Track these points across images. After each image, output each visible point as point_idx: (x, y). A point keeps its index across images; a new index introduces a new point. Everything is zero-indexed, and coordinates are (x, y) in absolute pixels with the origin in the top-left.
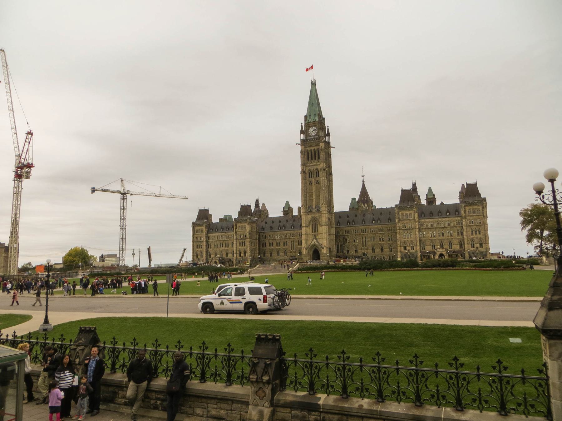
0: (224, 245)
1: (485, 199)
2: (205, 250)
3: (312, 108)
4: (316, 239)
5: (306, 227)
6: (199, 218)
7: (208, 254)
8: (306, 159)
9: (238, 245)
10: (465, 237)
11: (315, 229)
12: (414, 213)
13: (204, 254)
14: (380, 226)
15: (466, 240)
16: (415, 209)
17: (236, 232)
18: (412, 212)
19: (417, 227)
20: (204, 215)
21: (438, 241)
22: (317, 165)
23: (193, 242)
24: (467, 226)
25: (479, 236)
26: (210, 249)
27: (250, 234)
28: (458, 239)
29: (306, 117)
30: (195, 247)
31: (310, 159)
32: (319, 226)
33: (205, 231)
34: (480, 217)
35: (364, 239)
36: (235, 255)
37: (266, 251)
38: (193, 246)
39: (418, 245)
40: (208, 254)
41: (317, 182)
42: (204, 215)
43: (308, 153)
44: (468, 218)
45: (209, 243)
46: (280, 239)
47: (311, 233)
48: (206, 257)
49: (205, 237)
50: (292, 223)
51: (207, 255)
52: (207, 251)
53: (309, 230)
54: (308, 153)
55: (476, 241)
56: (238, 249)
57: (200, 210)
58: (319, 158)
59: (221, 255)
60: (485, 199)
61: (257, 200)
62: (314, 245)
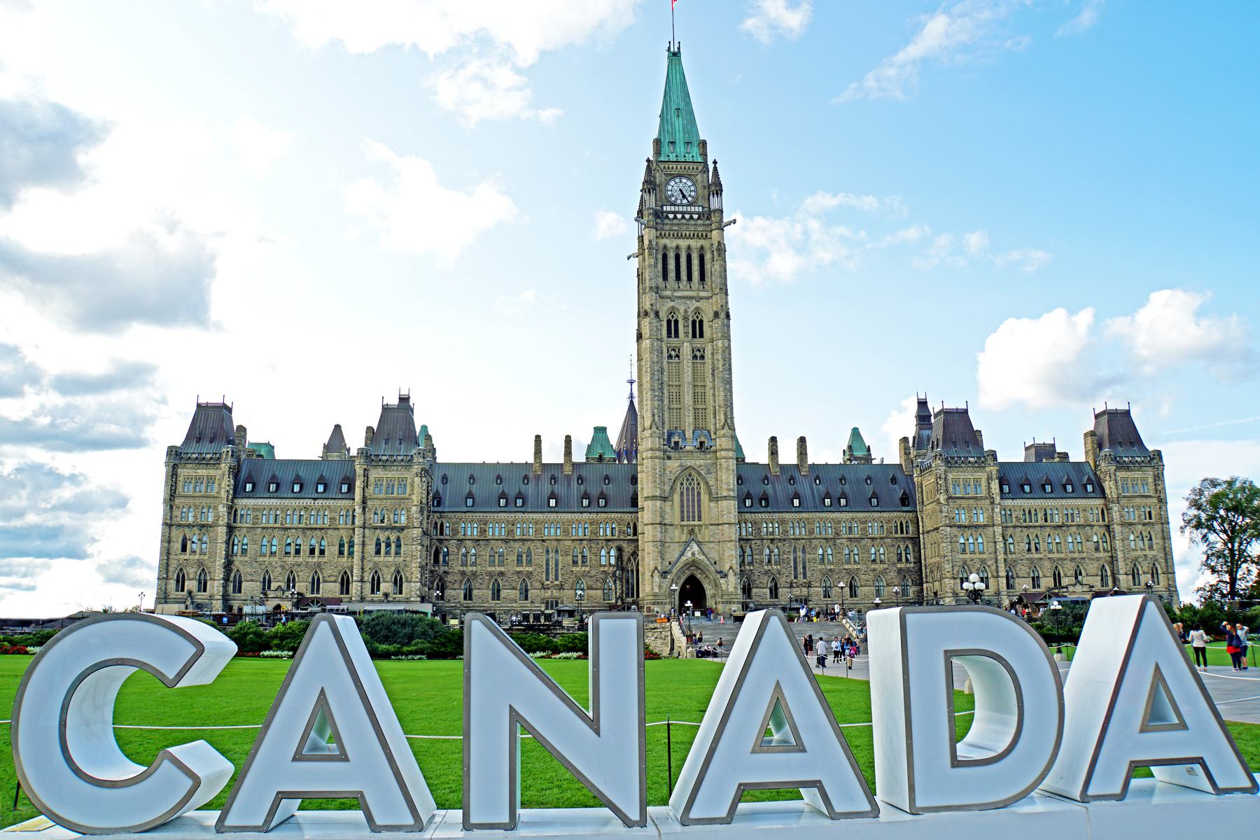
0: (305, 549)
1: (1158, 454)
2: (220, 561)
3: (679, 123)
4: (699, 544)
5: (664, 499)
6: (195, 434)
7: (232, 579)
8: (660, 274)
9: (371, 548)
10: (1120, 555)
11: (691, 510)
12: (989, 479)
13: (219, 573)
14: (851, 515)
15: (1121, 564)
16: (993, 470)
17: (364, 501)
18: (983, 476)
19: (998, 519)
20: (212, 424)
21: (1047, 564)
22: (699, 299)
23: (168, 525)
24: (1122, 524)
25: (1147, 552)
26: (238, 560)
27: (421, 511)
28: (1098, 559)
29: (657, 142)
30: (177, 546)
31: (672, 275)
32: (705, 498)
33: (227, 483)
34: (1149, 501)
35: (799, 554)
36: (355, 588)
37: (449, 578)
38: (167, 540)
39: (1003, 573)
40: (232, 579)
41: (698, 356)
42: (212, 424)
43: (665, 257)
44: (1123, 501)
45: (240, 538)
46: (506, 541)
47: (677, 521)
48: (225, 587)
49: (222, 510)
50: (546, 488)
51: (226, 579)
52: (228, 566)
53: (673, 512)
54: (665, 257)
55: (1144, 566)
56: (368, 566)
57: (199, 405)
58: (702, 277)
59: (291, 582)
60: (1158, 454)
61: (404, 400)
62: (693, 564)
